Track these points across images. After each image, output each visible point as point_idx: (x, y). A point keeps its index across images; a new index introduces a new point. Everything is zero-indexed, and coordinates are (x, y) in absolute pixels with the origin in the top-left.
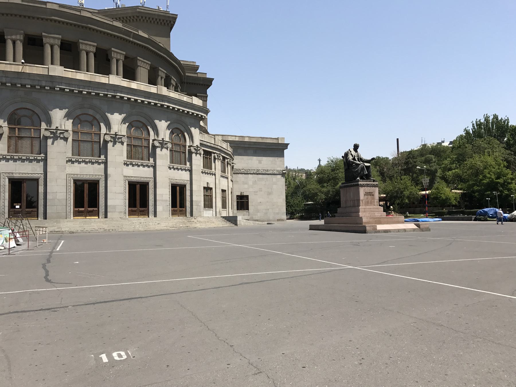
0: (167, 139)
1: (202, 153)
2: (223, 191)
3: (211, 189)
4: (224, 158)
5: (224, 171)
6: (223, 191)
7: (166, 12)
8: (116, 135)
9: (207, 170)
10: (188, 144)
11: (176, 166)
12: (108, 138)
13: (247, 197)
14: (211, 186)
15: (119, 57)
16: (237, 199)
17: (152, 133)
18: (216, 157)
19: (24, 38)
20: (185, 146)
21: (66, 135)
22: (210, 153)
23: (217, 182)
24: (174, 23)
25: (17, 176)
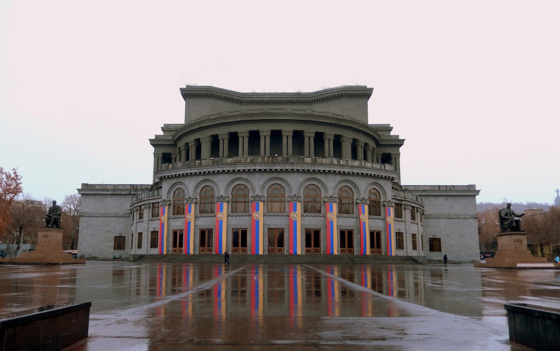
0: (367, 198)
1: (394, 205)
2: (414, 236)
3: (402, 233)
4: (413, 207)
5: (413, 218)
6: (414, 236)
7: (365, 87)
8: (331, 197)
9: (398, 219)
10: (382, 200)
11: (373, 217)
12: (326, 200)
13: (439, 240)
14: (402, 232)
15: (330, 138)
16: (430, 241)
17: (355, 194)
18: (406, 207)
19: (271, 134)
20: (379, 202)
21: (300, 199)
22: (401, 204)
23: (407, 227)
24: (371, 94)
25: (272, 227)
